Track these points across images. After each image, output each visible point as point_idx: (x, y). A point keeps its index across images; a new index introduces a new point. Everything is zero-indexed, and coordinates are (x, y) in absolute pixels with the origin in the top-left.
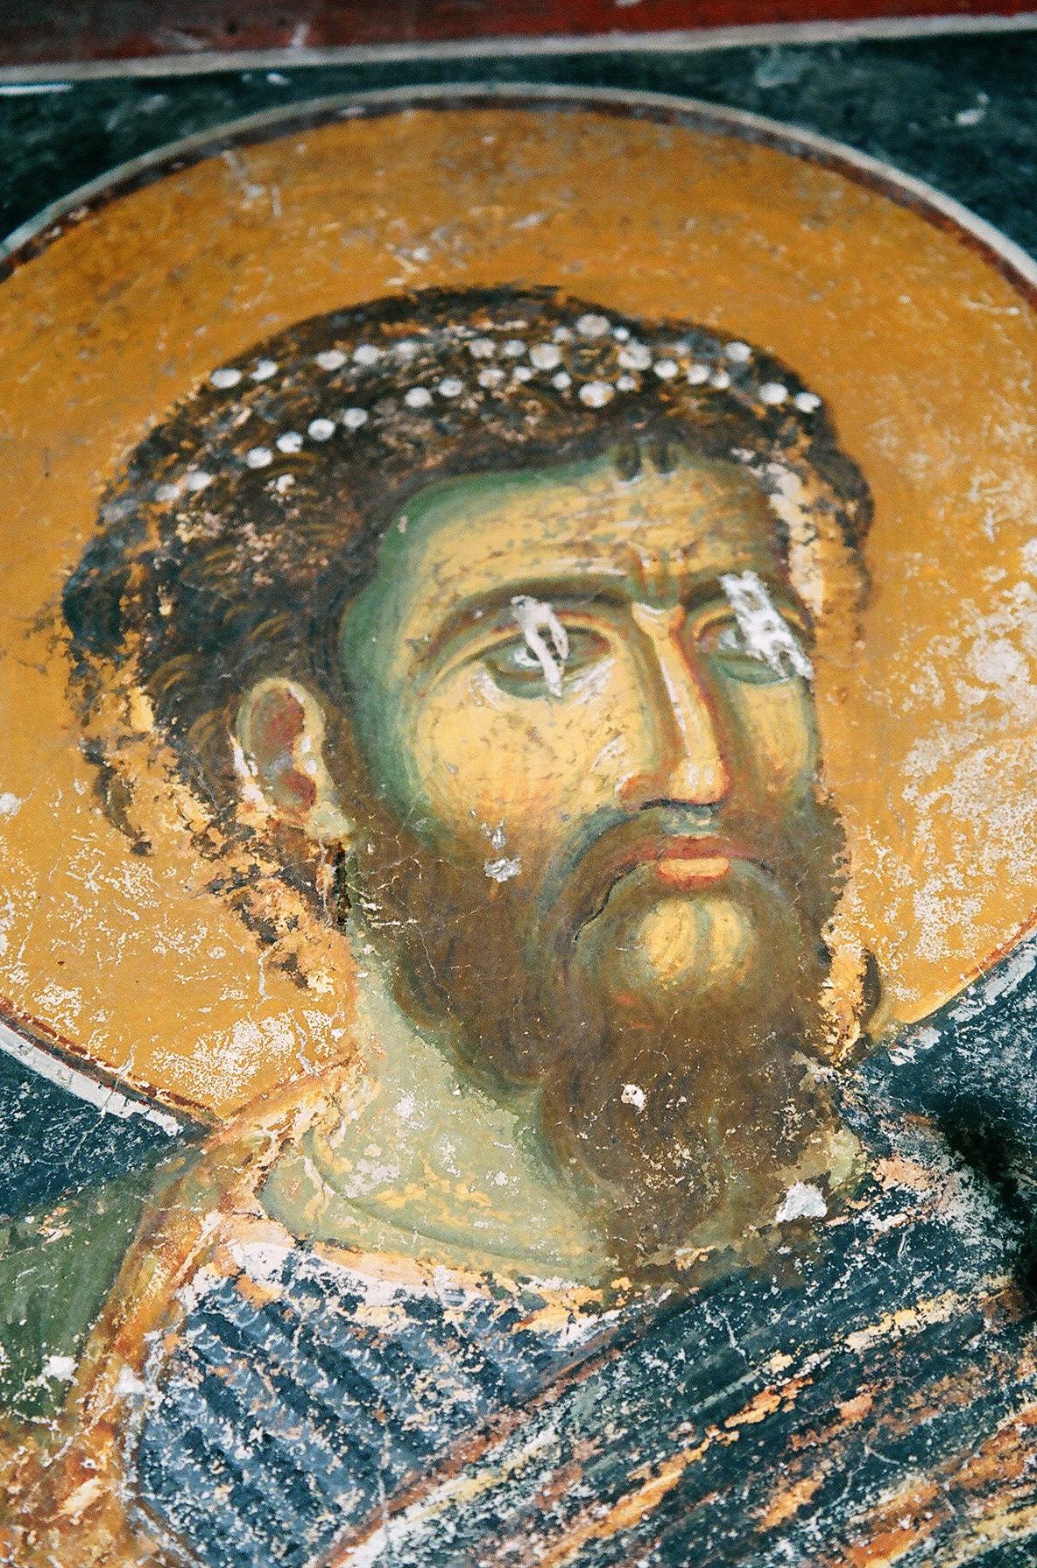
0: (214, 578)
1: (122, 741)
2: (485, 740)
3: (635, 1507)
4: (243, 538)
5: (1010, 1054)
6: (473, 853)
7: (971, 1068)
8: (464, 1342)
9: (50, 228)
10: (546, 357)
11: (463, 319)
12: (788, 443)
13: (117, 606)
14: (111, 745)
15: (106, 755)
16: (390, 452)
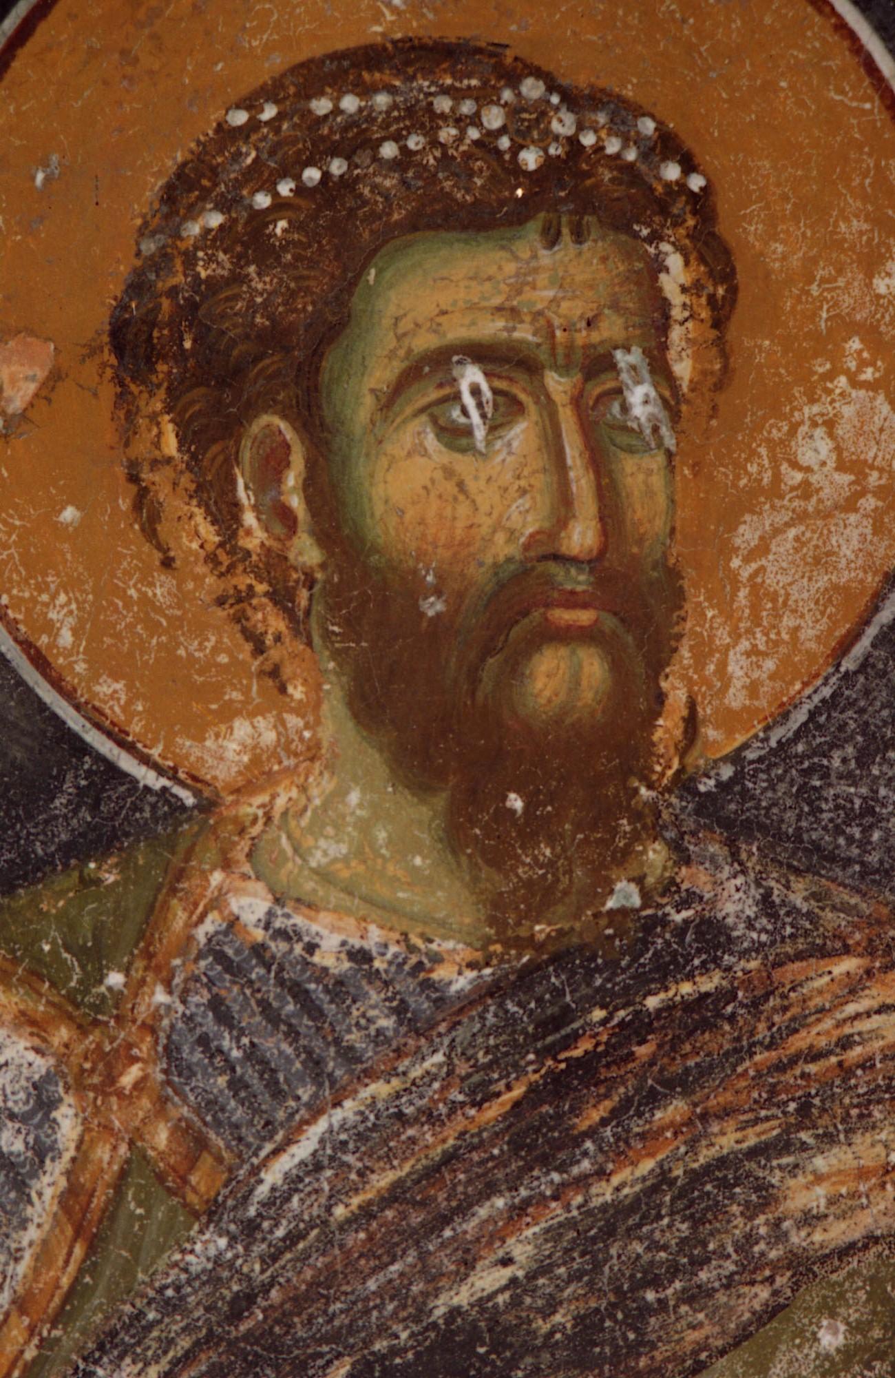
0: (223, 316)
1: (155, 464)
2: (425, 488)
3: (493, 1111)
4: (246, 279)
5: (782, 788)
6: (414, 590)
7: (753, 798)
8: (387, 984)
11: (428, 73)
13: (151, 337)
14: (146, 467)
15: (143, 476)
16: (365, 203)
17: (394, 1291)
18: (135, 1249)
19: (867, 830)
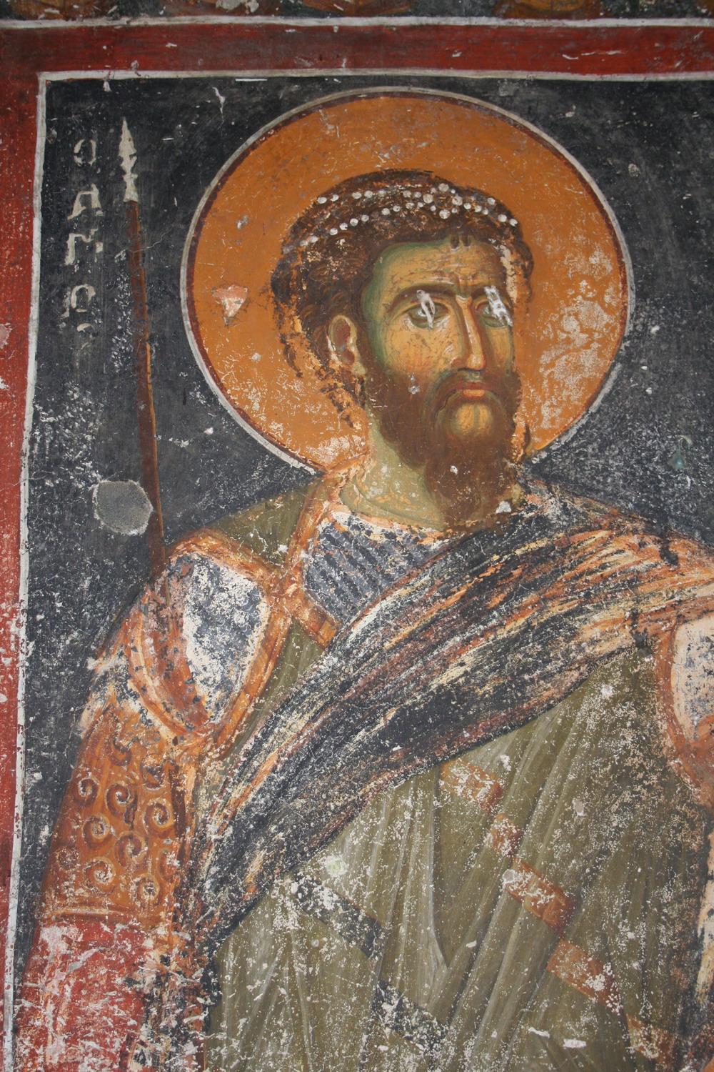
0: (319, 276)
1: (292, 336)
3: (453, 600)
4: (328, 262)
5: (568, 461)
6: (405, 383)
8: (403, 547)
9: (261, 137)
10: (429, 199)
12: (507, 237)
16: (377, 232)
17: (414, 678)
18: (297, 664)
19: (605, 478)
